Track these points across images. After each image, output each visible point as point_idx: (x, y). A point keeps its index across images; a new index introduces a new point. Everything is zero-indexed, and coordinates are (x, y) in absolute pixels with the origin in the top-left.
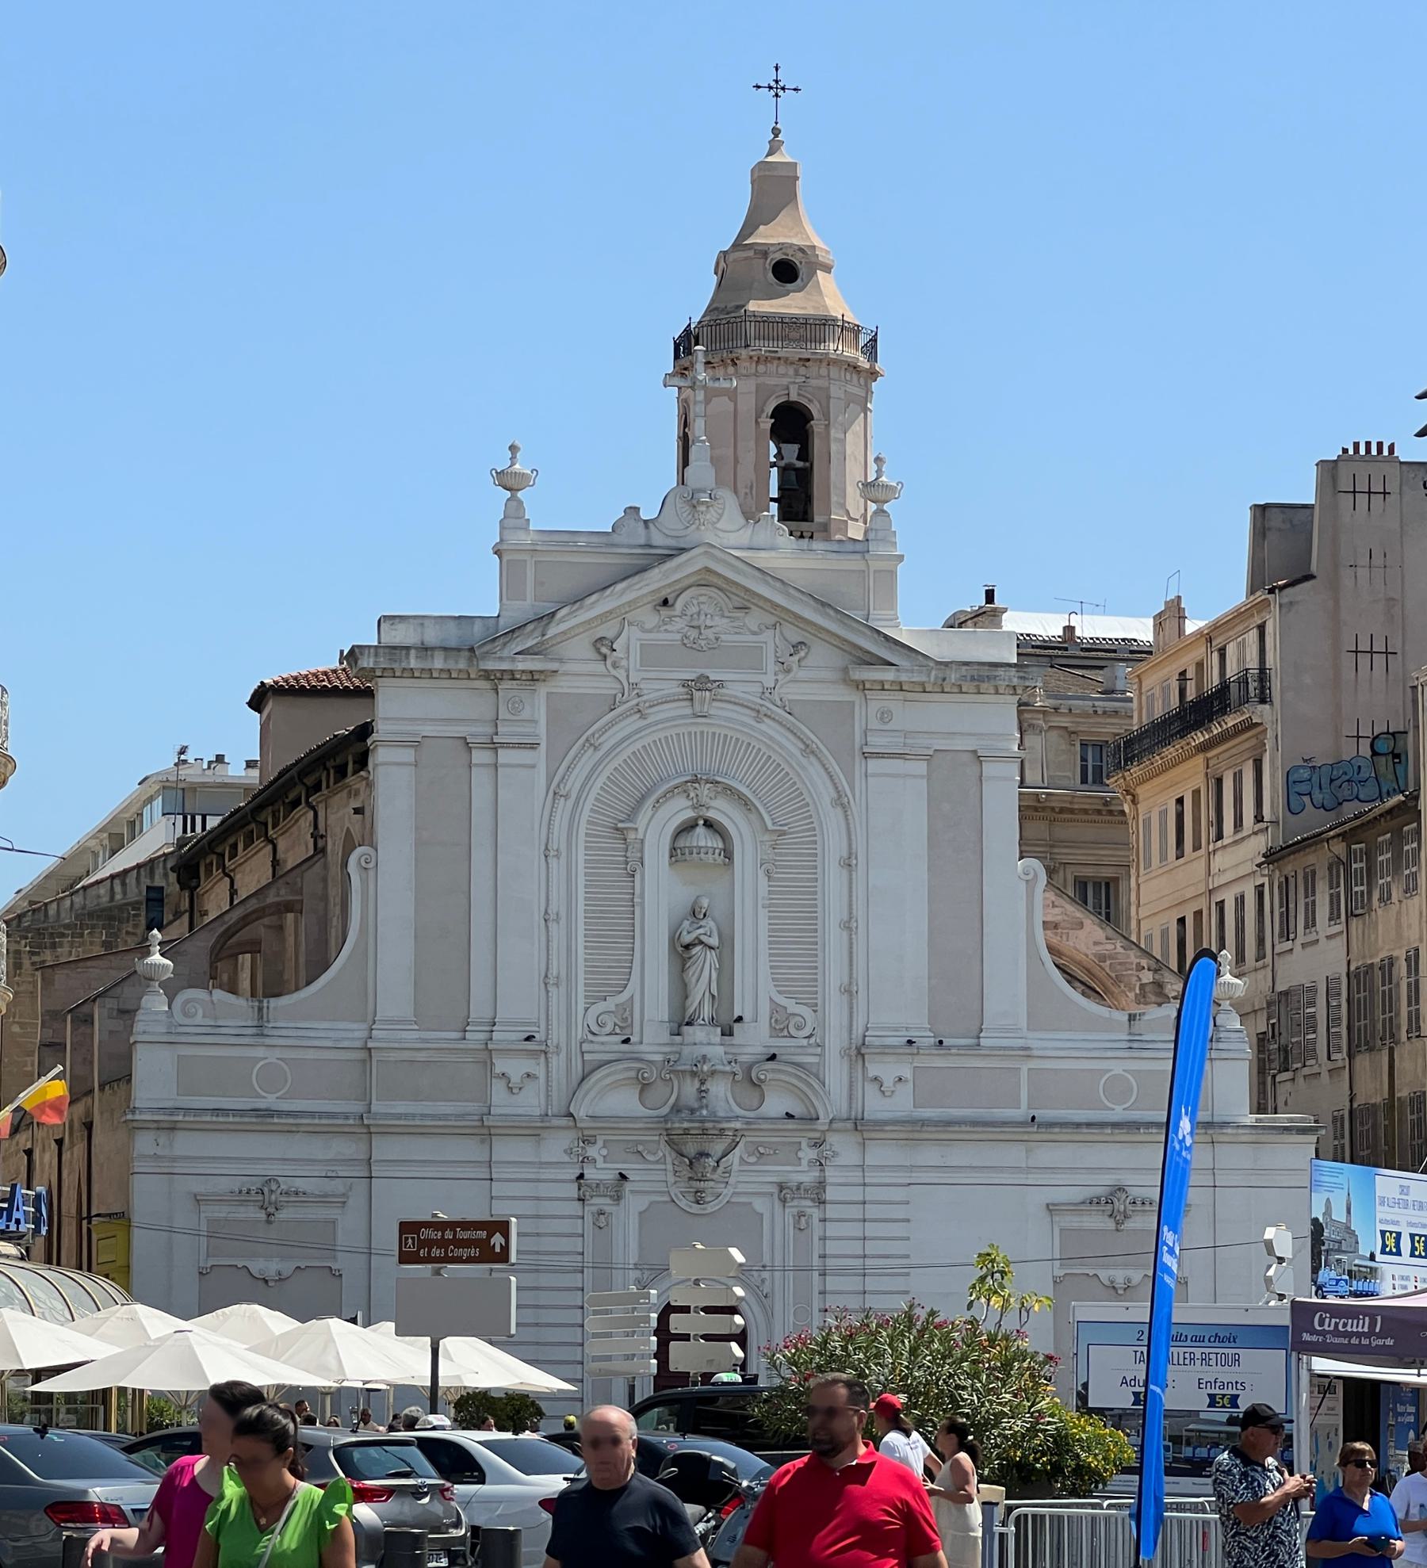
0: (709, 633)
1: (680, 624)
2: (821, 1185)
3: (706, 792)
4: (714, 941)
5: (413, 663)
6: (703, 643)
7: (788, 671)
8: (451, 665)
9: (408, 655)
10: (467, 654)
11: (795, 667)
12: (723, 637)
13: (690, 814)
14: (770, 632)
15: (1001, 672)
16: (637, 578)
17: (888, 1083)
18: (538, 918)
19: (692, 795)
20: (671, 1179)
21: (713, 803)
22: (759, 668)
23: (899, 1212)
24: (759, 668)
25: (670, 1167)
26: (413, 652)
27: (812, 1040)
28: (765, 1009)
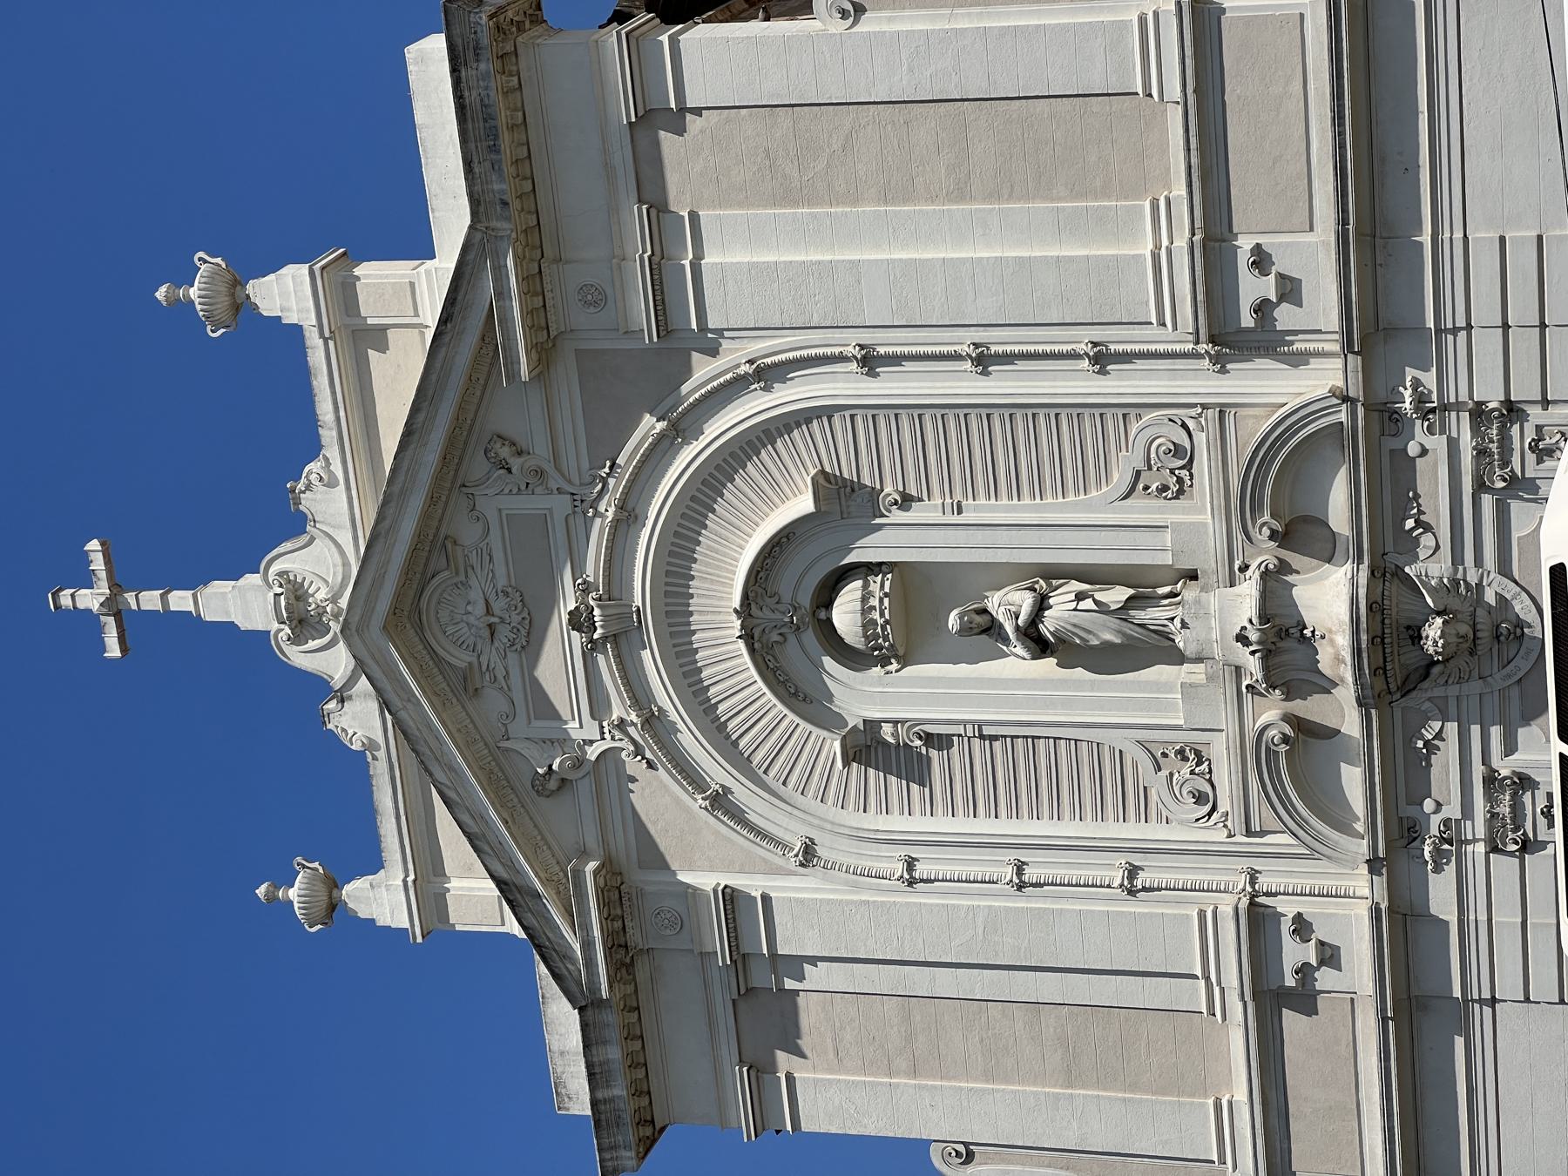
0: (498, 605)
1: (490, 656)
2: (1479, 413)
3: (767, 613)
4: (1026, 602)
5: (619, 1090)
6: (516, 619)
7: (540, 473)
8: (614, 1034)
9: (612, 1100)
10: (589, 1012)
11: (531, 462)
12: (502, 582)
13: (810, 638)
14: (480, 502)
15: (471, 97)
16: (423, 749)
17: (1268, 287)
18: (1020, 903)
19: (775, 637)
20: (1475, 686)
21: (787, 597)
22: (544, 519)
23: (1522, 262)
24: (544, 519)
25: (1453, 690)
26: (600, 1095)
27: (1191, 424)
28: (1142, 510)
